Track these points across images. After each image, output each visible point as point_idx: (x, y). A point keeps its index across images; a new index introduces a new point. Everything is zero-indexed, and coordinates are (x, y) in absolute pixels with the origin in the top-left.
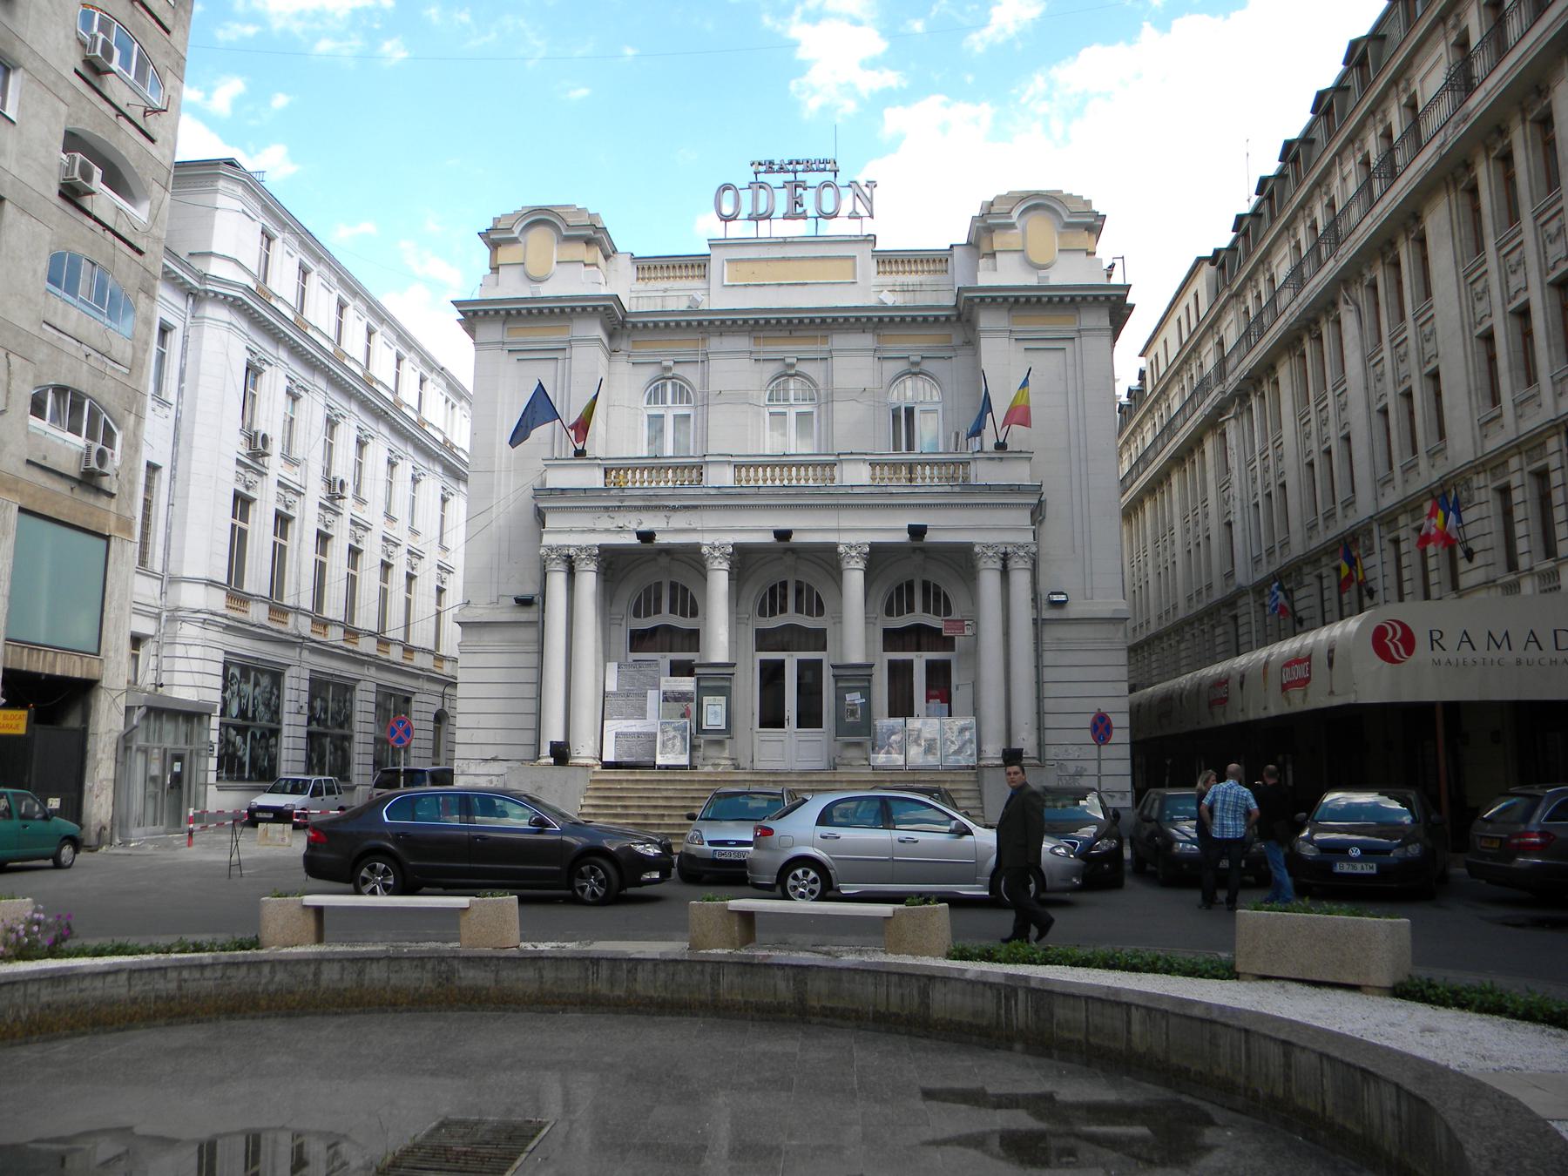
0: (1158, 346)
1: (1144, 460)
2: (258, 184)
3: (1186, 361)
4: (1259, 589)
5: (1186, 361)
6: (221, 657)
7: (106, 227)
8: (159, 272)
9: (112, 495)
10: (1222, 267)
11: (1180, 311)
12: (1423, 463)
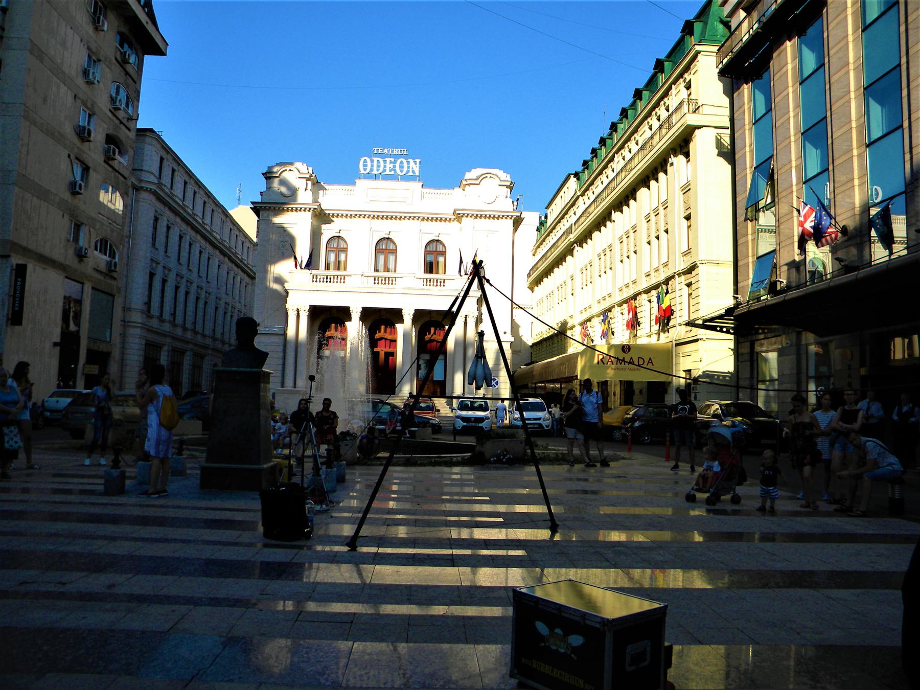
2: (160, 137)
6: (144, 342)
7: (116, 171)
8: (129, 184)
9: (115, 279)
10: (578, 179)
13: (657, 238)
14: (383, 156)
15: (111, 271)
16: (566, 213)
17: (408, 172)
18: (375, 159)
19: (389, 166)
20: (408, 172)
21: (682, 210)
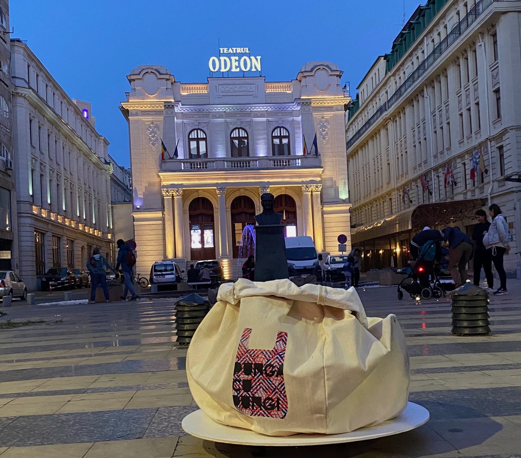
0: (363, 86)
1: (359, 133)
3: (375, 96)
4: (398, 189)
5: (375, 96)
10: (388, 61)
11: (372, 74)
12: (445, 152)
13: (469, 110)
14: (229, 55)
15: (7, 169)
16: (378, 92)
17: (251, 68)
18: (222, 58)
19: (235, 64)
20: (251, 68)
21: (490, 85)
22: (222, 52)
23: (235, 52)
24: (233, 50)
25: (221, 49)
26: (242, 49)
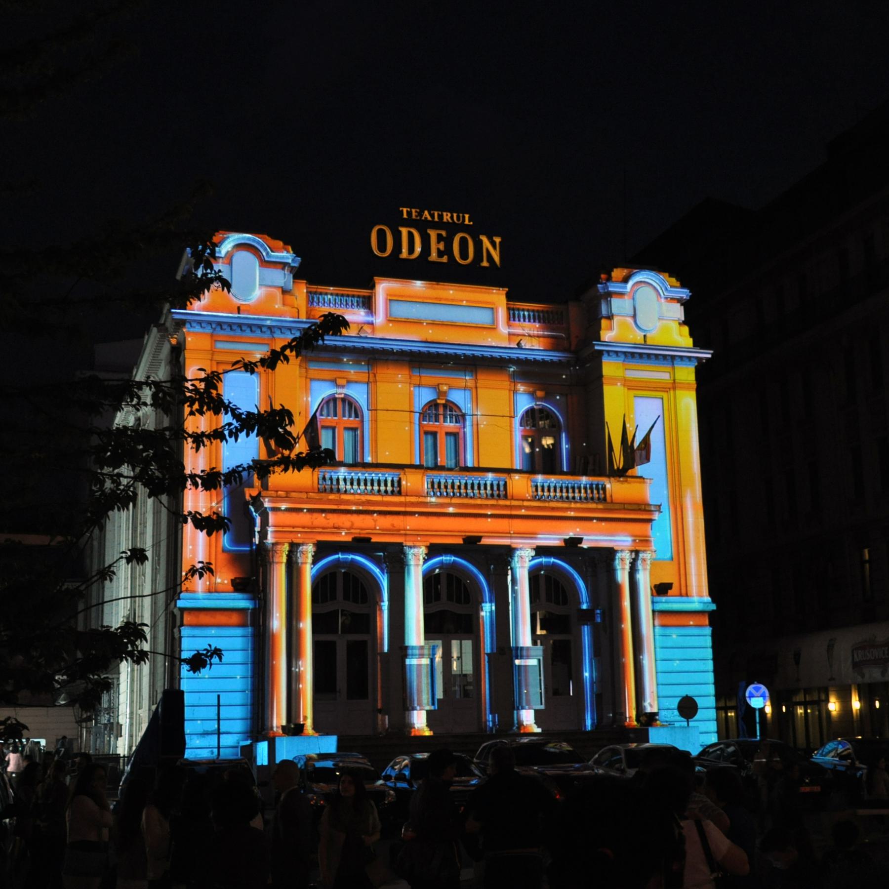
19: (435, 246)
22: (405, 216)
23: (436, 219)
24: (432, 216)
25: (405, 210)
26: (455, 215)
